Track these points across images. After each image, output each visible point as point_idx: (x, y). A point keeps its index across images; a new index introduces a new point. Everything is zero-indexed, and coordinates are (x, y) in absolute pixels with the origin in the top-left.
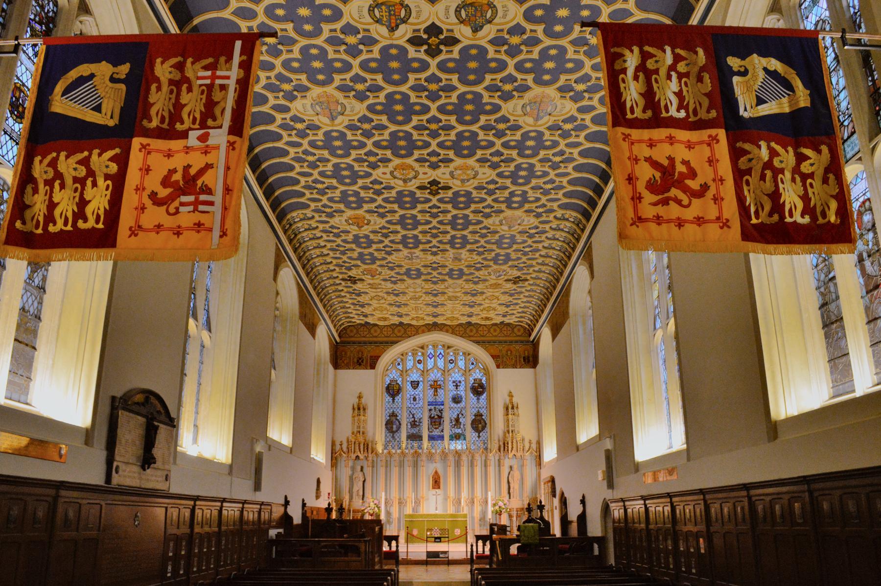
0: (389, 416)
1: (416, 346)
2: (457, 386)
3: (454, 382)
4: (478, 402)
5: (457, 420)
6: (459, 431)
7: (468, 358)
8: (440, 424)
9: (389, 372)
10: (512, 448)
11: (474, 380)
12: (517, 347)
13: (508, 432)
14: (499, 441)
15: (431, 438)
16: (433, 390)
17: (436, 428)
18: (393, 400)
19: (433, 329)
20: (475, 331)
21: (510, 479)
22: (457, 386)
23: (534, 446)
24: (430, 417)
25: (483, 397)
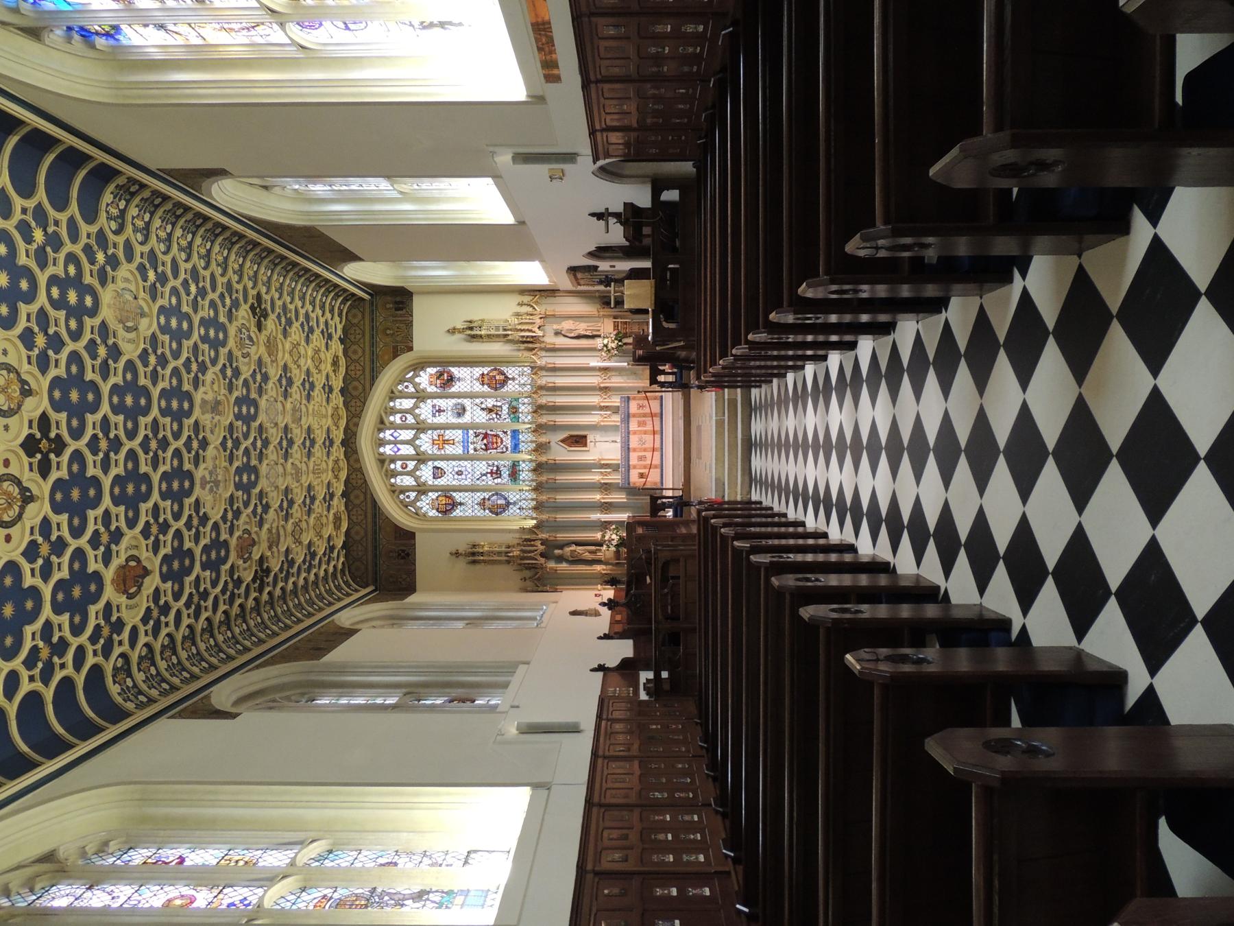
0: (484, 510)
1: (380, 472)
2: (440, 411)
3: (434, 415)
4: (463, 380)
7: (397, 393)
14: (519, 350)
16: (446, 446)
18: (461, 504)
19: (353, 446)
21: (572, 335)
22: (440, 411)
23: (526, 299)
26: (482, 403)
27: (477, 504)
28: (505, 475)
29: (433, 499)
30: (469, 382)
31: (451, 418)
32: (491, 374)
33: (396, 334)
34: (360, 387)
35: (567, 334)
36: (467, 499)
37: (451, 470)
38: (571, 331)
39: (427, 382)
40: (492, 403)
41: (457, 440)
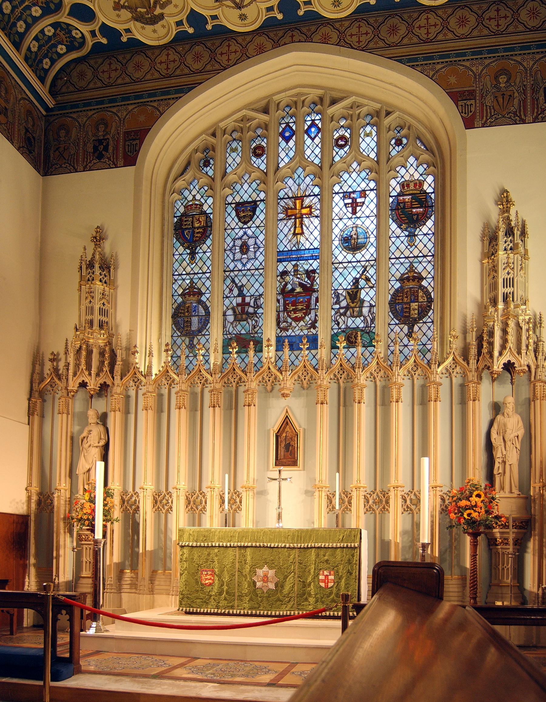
0: (183, 295)
2: (354, 205)
3: (346, 195)
4: (411, 244)
6: (359, 322)
8: (308, 306)
10: (505, 341)
11: (402, 185)
12: (528, 63)
13: (494, 302)
14: (465, 332)
16: (290, 223)
17: (297, 320)
18: (193, 254)
19: (287, 39)
20: (403, 30)
21: (494, 435)
22: (354, 205)
24: (283, 292)
25: (425, 229)
26: (367, 280)
29: (202, 205)
30: (407, 253)
31: (341, 225)
32: (421, 294)
33: (499, 94)
34: (395, 39)
35: (495, 425)
36: (200, 264)
37: (249, 232)
38: (503, 434)
39: (407, 177)
40: (367, 299)
41: (302, 239)
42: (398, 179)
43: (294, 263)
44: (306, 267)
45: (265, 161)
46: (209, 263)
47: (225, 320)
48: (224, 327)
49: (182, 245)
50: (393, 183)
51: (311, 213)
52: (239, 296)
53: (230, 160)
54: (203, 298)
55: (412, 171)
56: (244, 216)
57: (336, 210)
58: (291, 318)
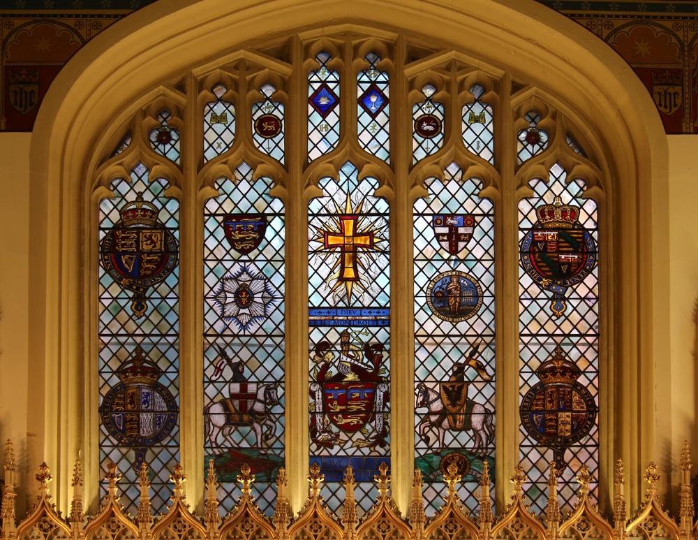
0: (120, 372)
3: (438, 219)
5: (455, 390)
9: (112, 168)
15: (329, 470)
17: (349, 429)
18: (139, 302)
26: (480, 368)
27: (139, 348)
28: (236, 437)
29: (156, 212)
30: (550, 328)
31: (430, 271)
32: (576, 398)
36: (155, 318)
37: (253, 269)
39: (549, 199)
42: (533, 201)
43: (341, 329)
44: (365, 339)
45: (282, 145)
46: (172, 318)
47: (208, 422)
48: (207, 434)
49: (117, 281)
50: (524, 206)
51: (372, 245)
52: (234, 380)
53: (210, 136)
54: (163, 381)
55: (557, 188)
56: (242, 240)
57: (420, 243)
58: (341, 427)
